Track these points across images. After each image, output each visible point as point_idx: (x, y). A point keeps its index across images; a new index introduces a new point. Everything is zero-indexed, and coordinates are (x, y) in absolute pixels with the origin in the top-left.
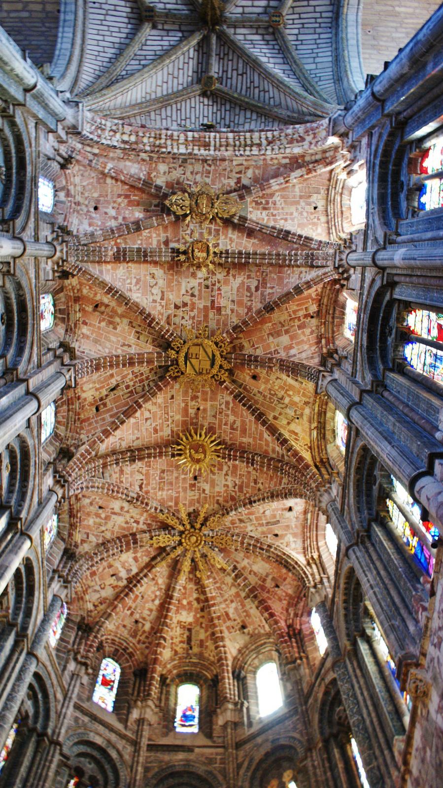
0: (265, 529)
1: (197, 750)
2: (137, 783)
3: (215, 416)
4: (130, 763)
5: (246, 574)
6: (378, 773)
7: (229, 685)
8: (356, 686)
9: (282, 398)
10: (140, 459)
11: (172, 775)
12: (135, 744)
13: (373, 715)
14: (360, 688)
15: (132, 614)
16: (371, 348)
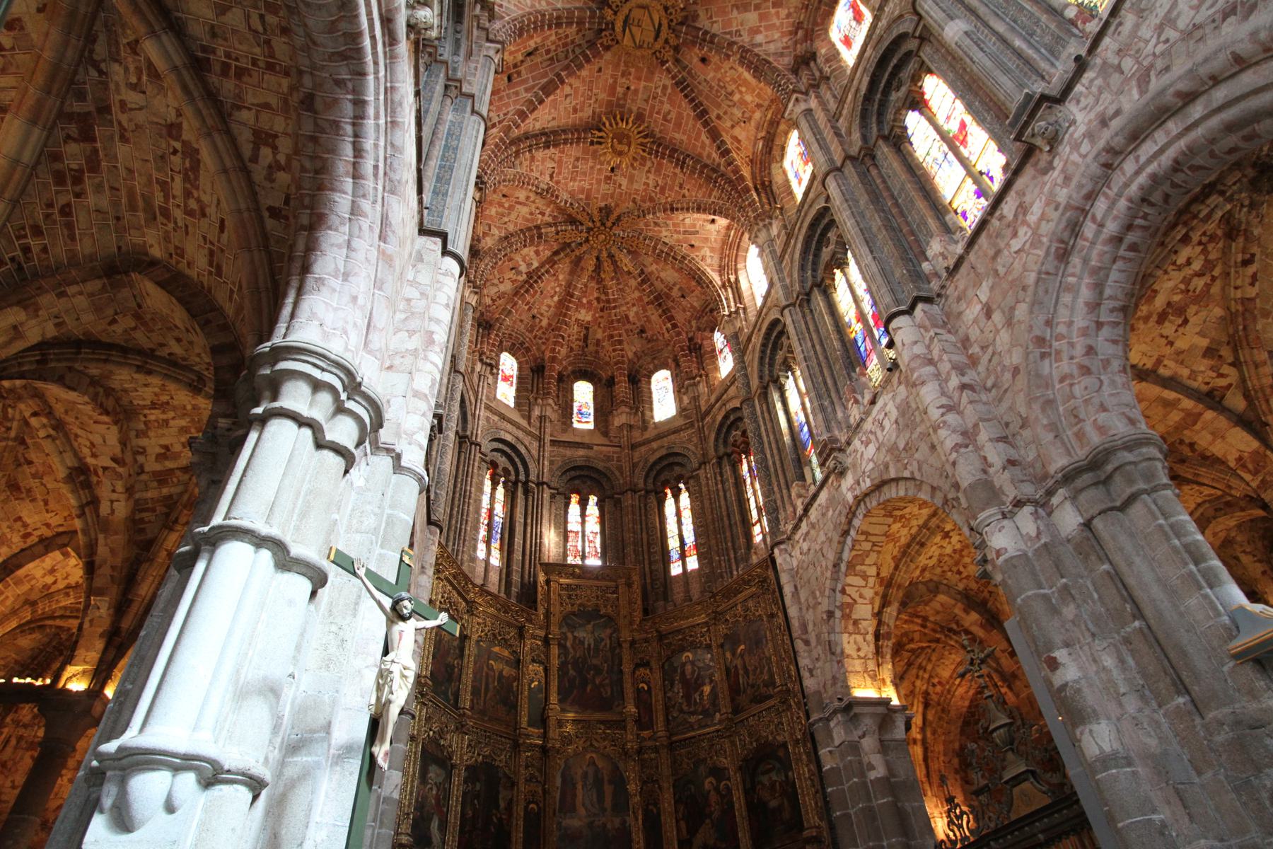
0: (681, 237)
3: (647, 101)
5: (653, 278)
7: (622, 388)
8: (763, 429)
9: (732, 94)
10: (555, 146)
11: (574, 468)
12: (540, 439)
13: (777, 458)
14: (766, 430)
15: (530, 309)
16: (868, 98)
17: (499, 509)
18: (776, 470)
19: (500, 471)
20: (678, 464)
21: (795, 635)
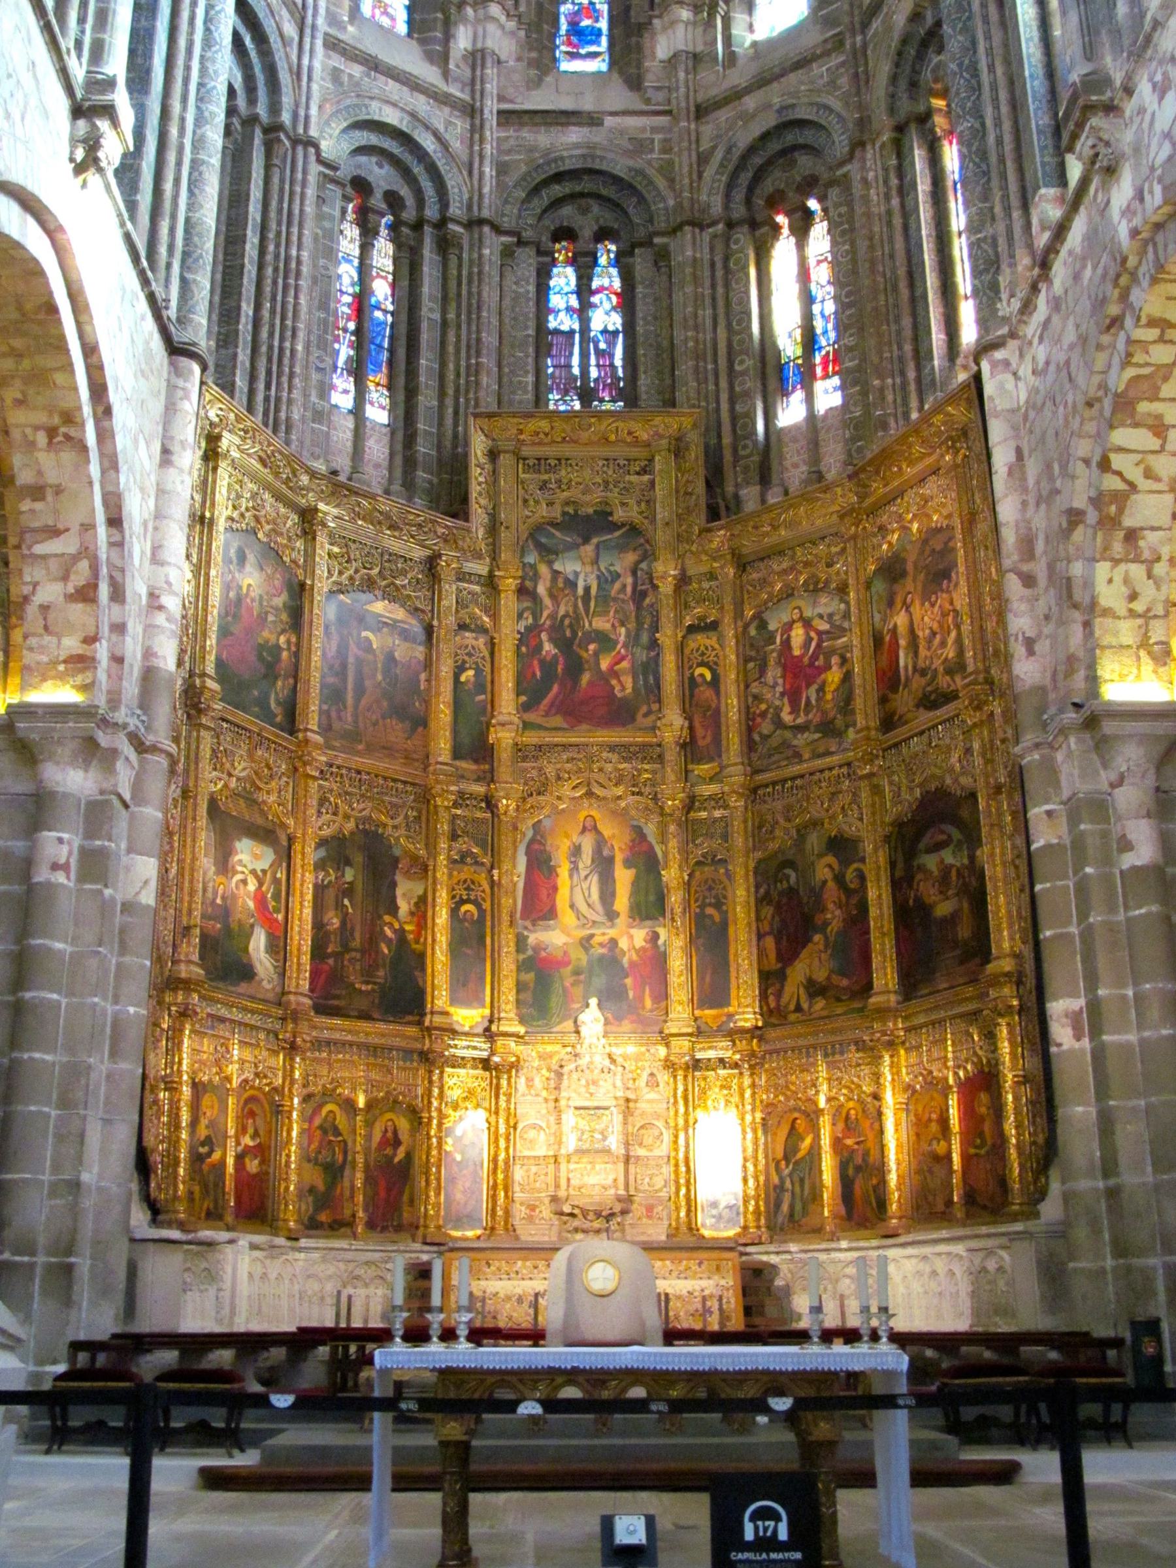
1: (609, 121)
2: (486, 201)
4: (465, 157)
6: (990, 251)
11: (558, 177)
12: (471, 111)
13: (1007, 126)
14: (989, 52)
17: (381, 290)
18: (1002, 160)
19: (377, 201)
20: (806, 148)
21: (1007, 563)
